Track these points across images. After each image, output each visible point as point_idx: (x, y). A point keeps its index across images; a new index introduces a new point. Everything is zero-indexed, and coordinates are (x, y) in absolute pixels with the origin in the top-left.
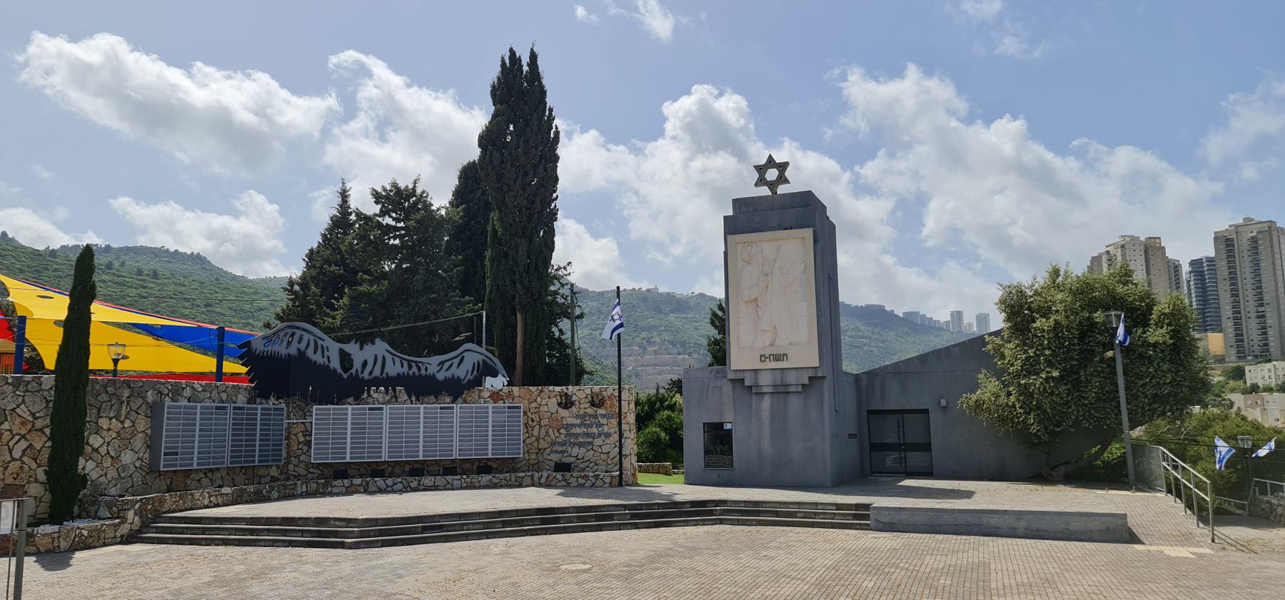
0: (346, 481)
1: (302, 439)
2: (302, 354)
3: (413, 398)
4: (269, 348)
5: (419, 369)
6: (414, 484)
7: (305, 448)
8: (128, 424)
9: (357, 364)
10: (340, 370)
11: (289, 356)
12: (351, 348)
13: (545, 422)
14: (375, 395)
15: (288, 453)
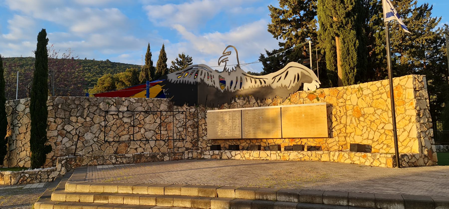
0: (211, 152)
1: (204, 128)
2: (202, 80)
3: (259, 101)
5: (261, 83)
6: (247, 156)
7: (205, 133)
8: (88, 119)
9: (228, 84)
10: (219, 88)
11: (197, 83)
13: (349, 112)
14: (238, 101)
15: (198, 135)
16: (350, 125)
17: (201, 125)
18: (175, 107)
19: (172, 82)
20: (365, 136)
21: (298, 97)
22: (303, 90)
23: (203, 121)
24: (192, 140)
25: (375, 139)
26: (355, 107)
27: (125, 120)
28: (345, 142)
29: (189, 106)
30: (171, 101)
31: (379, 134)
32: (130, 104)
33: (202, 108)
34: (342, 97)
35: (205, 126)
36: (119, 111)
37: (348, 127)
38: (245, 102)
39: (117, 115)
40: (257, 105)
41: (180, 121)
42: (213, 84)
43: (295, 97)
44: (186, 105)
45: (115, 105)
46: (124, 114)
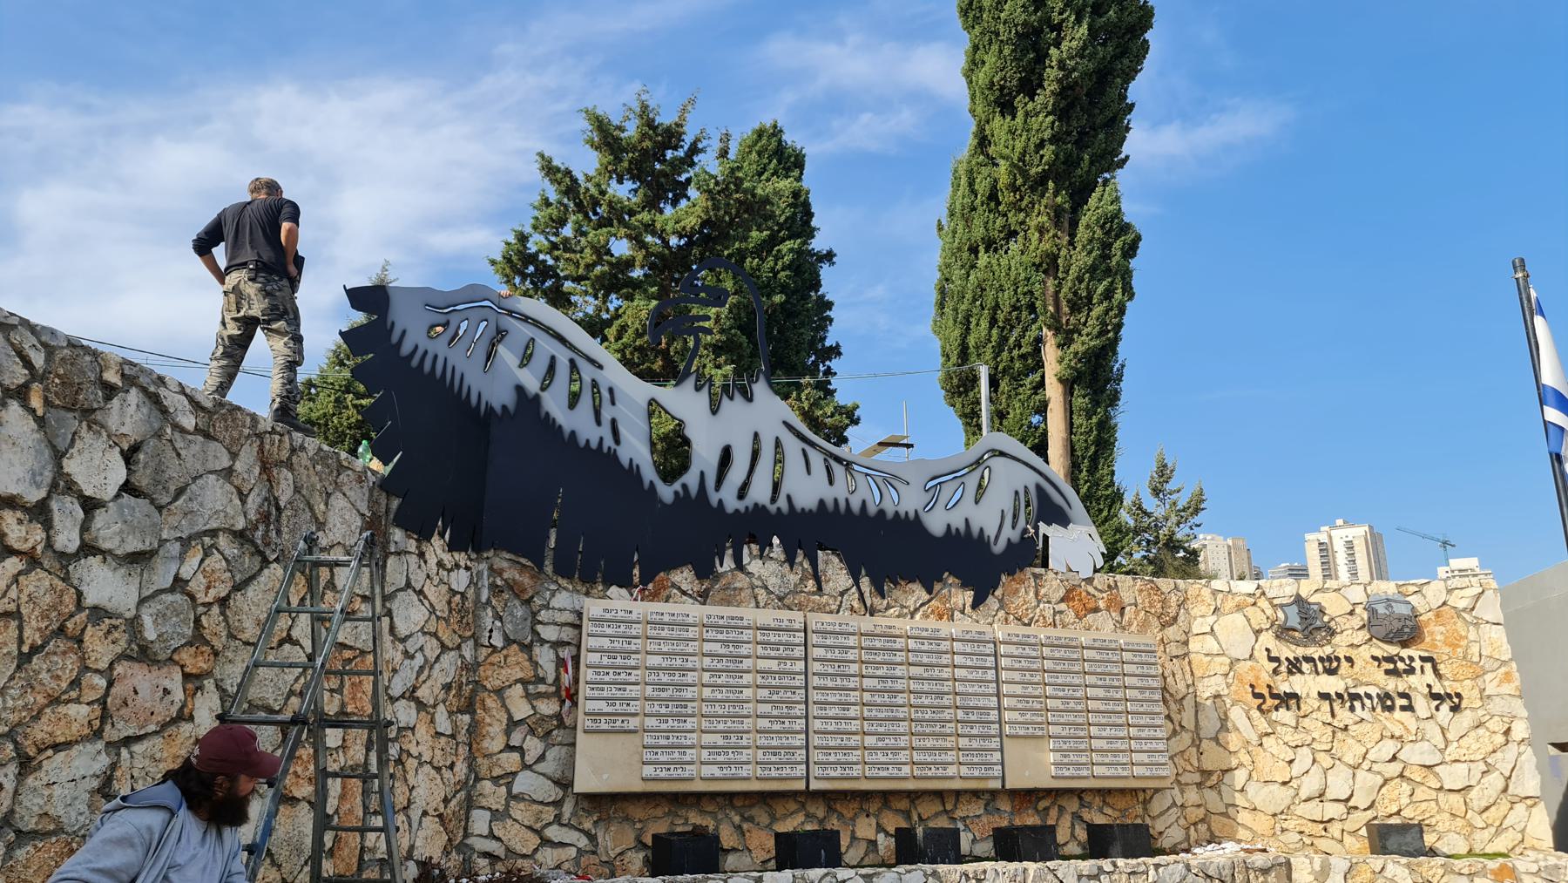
1: (521, 710)
4: (439, 347)
10: (649, 474)
12: (684, 402)
14: (755, 566)
16: (1216, 739)
17: (499, 692)
18: (397, 535)
19: (406, 349)
20: (1310, 786)
21: (1032, 594)
22: (1045, 564)
23: (517, 667)
24: (446, 801)
25: (1360, 800)
26: (1243, 667)
27: (104, 585)
28: (1201, 812)
29: (452, 547)
30: (386, 485)
31: (1380, 780)
32: (158, 435)
33: (511, 574)
34: (1175, 619)
35: (528, 696)
36: (63, 484)
37: (1205, 745)
38: (794, 578)
39: (40, 513)
40: (856, 604)
41: (411, 646)
42: (609, 442)
43: (1021, 592)
44: (442, 535)
45: (36, 402)
46: (100, 518)
